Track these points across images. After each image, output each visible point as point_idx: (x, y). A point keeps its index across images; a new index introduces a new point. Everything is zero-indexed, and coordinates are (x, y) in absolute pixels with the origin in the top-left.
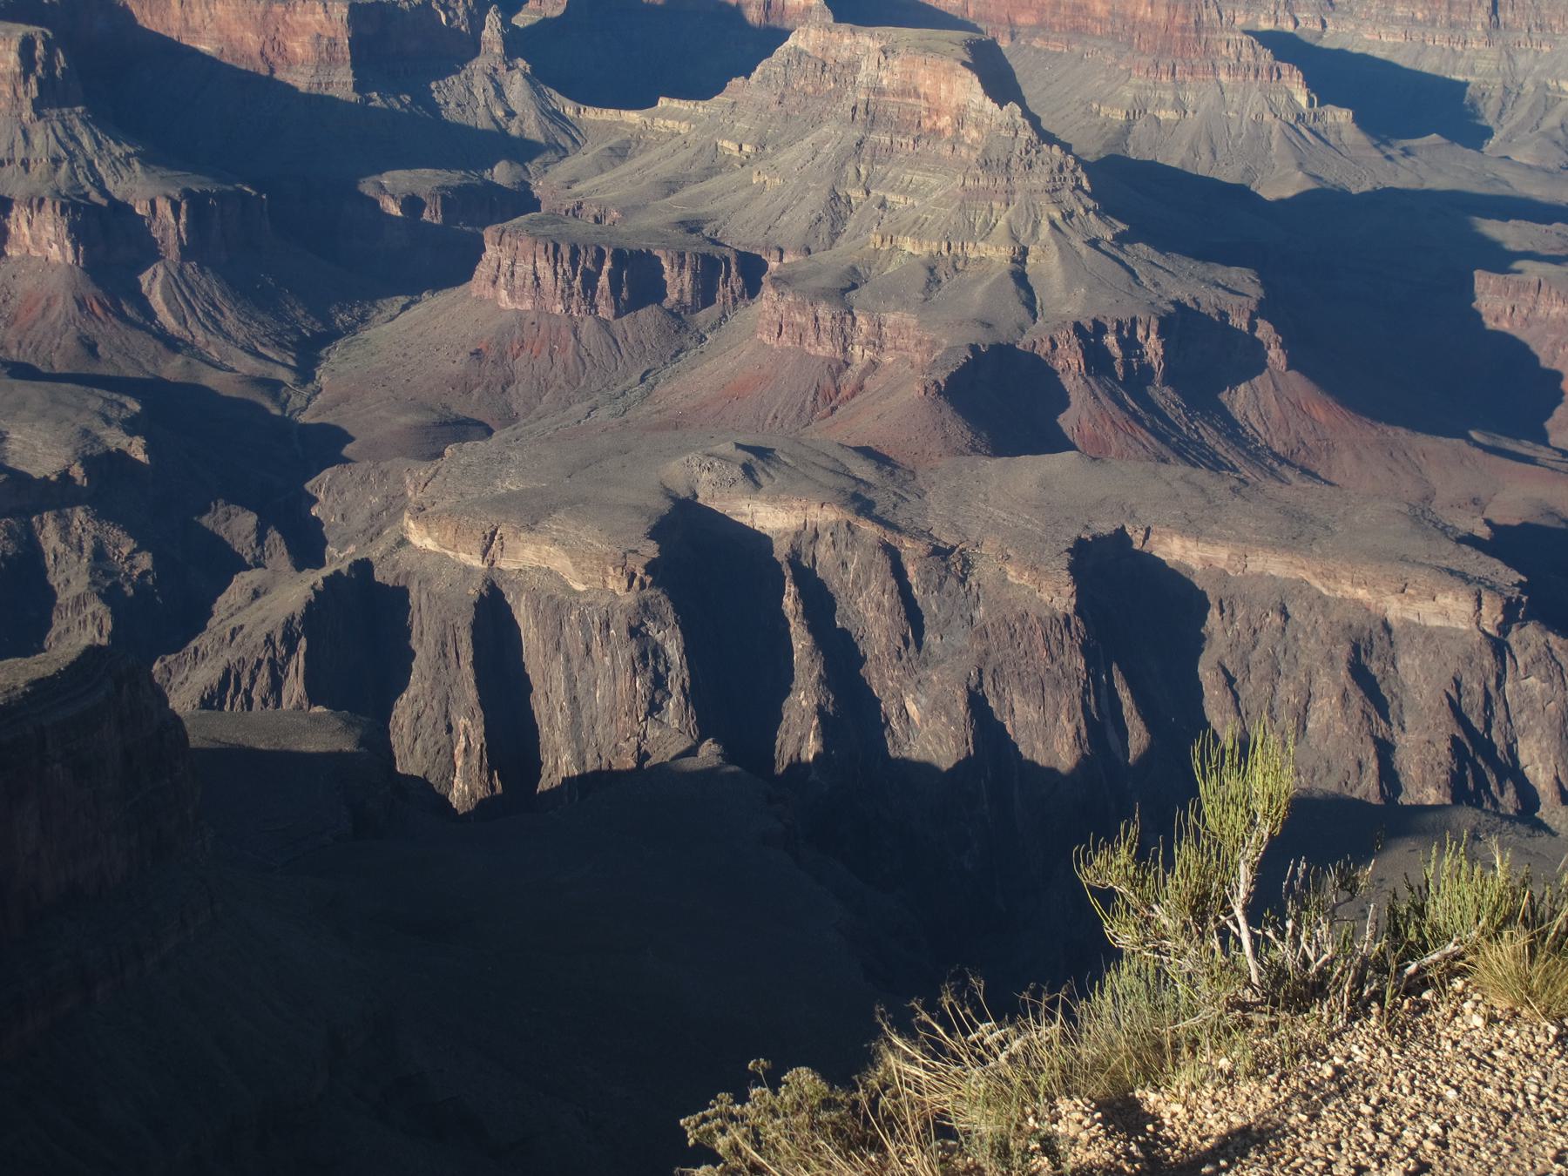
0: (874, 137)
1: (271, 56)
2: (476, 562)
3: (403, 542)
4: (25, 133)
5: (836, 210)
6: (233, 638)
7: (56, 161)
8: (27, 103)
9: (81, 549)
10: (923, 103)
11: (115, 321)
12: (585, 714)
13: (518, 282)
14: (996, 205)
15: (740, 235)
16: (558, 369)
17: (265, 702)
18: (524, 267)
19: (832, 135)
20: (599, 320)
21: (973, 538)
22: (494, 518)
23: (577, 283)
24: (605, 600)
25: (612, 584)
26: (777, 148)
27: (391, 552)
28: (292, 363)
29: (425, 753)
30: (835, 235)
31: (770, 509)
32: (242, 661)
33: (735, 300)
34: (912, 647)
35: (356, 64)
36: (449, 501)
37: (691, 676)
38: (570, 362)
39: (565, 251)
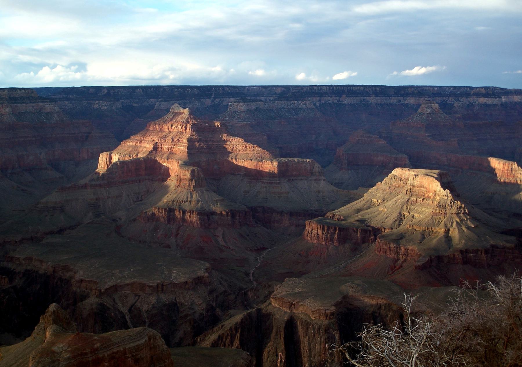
0: (412, 198)
3: (270, 304)
4: (191, 194)
8: (192, 186)
10: (425, 190)
12: (313, 353)
14: (441, 217)
15: (375, 223)
18: (314, 232)
19: (401, 198)
24: (319, 322)
26: (387, 201)
29: (270, 361)
30: (400, 225)
32: (223, 334)
33: (372, 242)
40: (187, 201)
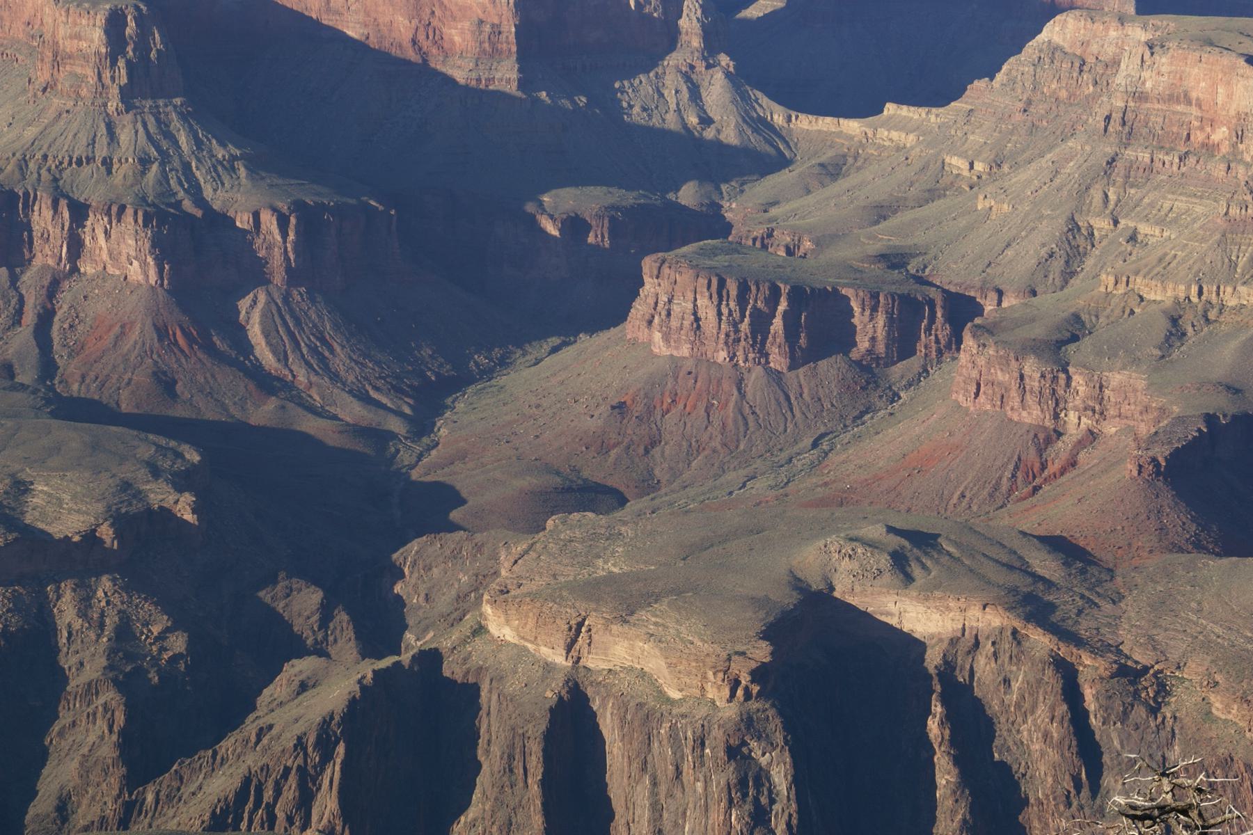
0: (1129, 153)
1: (425, 44)
2: (558, 658)
3: (480, 630)
4: (110, 128)
5: (1074, 246)
6: (259, 740)
7: (145, 162)
8: (114, 91)
9: (102, 625)
10: (1194, 111)
11: (201, 355)
13: (674, 323)
15: (952, 272)
16: (715, 429)
17: (290, 820)
18: (682, 306)
19: (1080, 152)
20: (769, 371)
21: (1174, 656)
22: (582, 606)
23: (745, 326)
24: (702, 711)
25: (711, 693)
26: (1016, 166)
27: (464, 642)
28: (407, 411)
30: (1069, 274)
31: (921, 608)
32: (266, 768)
33: (940, 353)
34: (1085, 792)
35: (524, 57)
36: (539, 583)
37: (799, 812)
38: (730, 422)
39: (732, 288)
40: (90, 160)
